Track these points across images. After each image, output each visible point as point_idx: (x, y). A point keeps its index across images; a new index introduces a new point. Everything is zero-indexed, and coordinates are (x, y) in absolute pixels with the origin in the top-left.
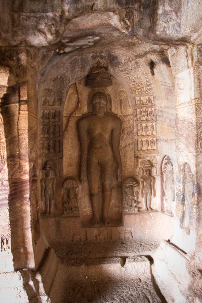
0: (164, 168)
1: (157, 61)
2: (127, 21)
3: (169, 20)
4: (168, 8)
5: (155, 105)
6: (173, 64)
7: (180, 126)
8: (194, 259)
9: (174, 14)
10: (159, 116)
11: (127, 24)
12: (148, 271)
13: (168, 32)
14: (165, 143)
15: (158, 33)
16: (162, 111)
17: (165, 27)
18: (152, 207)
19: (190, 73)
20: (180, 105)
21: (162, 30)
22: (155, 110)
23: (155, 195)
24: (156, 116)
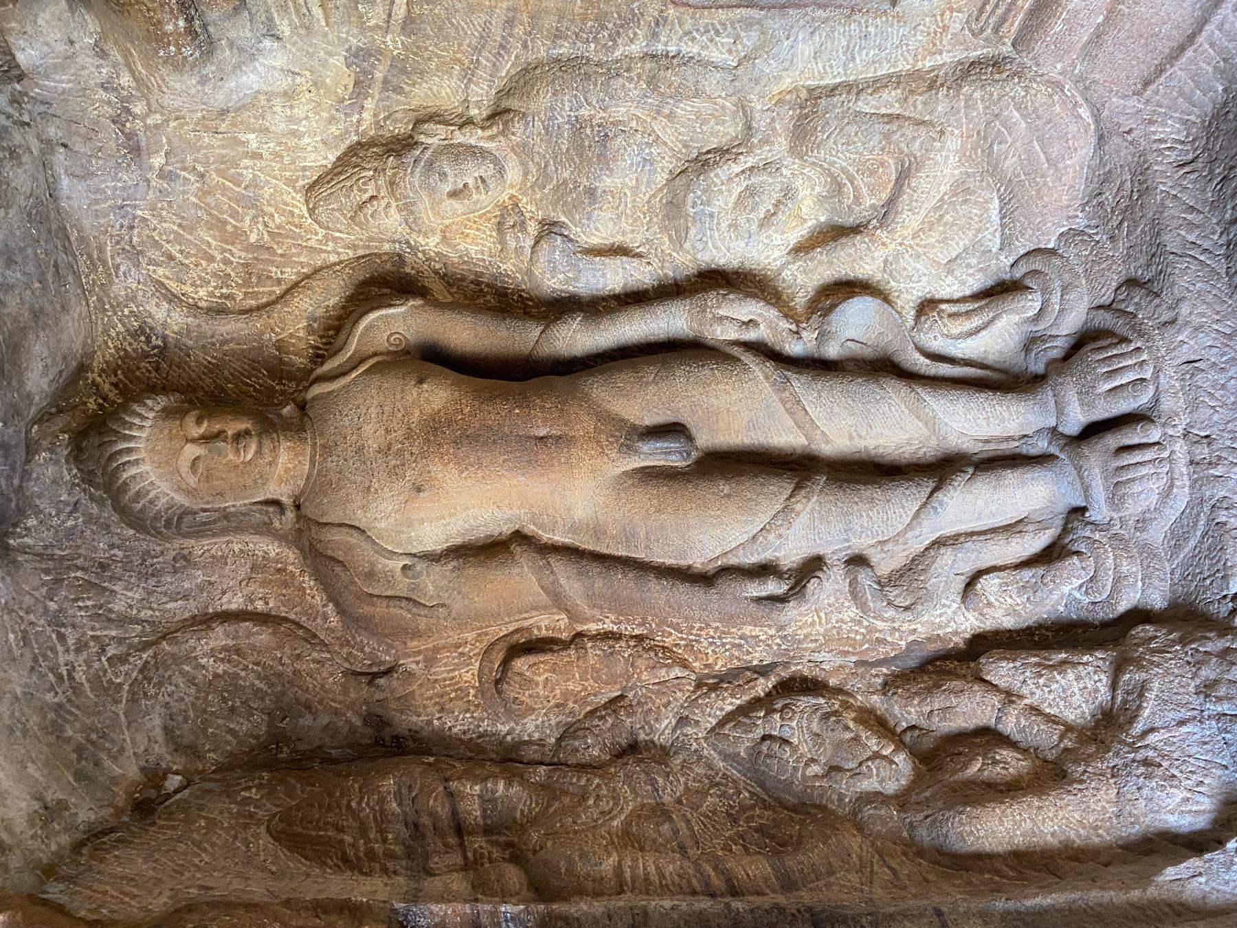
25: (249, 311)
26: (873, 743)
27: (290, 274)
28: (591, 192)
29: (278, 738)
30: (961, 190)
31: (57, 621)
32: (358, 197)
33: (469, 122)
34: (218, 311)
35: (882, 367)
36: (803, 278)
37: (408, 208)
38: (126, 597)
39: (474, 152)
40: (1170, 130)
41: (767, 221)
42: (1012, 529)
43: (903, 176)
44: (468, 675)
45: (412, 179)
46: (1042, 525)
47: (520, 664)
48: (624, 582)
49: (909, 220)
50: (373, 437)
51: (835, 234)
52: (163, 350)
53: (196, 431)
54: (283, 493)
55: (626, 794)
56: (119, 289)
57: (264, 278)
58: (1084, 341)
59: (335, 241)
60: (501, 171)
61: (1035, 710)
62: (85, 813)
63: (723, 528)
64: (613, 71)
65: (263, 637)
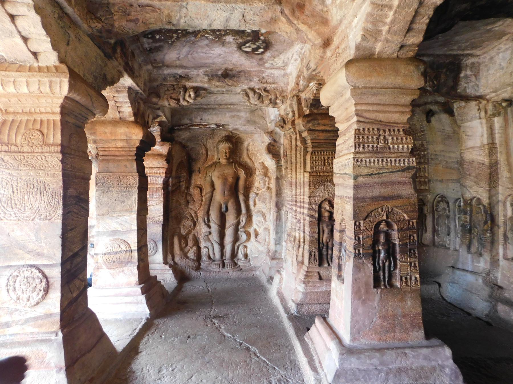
0: (436, 206)
1: (438, 111)
2: (435, 81)
3: (469, 81)
4: (469, 73)
5: (427, 149)
6: (458, 114)
7: (467, 167)
8: (489, 275)
9: (473, 77)
10: (432, 159)
11: (433, 83)
12: (437, 292)
13: (468, 91)
14: (438, 183)
15: (459, 91)
16: (436, 155)
17: (465, 87)
18: (423, 242)
19: (481, 123)
20: (468, 149)
21: (463, 89)
22: (428, 153)
23: (426, 231)
24: (428, 159)
25: (248, 154)
26: (187, 231)
27: (253, 159)
28: (260, 200)
29: (192, 159)
30: (259, 251)
31: (206, 135)
32: (260, 169)
33: (269, 184)
34: (248, 150)
35: (236, 239)
36: (251, 230)
37: (258, 175)
38: (210, 141)
39: (265, 185)
40: (258, 273)
41: (257, 224)
42: (214, 253)
43: (260, 242)
44: (199, 183)
45: (261, 177)
46: (214, 257)
47: (199, 189)
48: (208, 202)
49: (256, 244)
50: (226, 172)
51: (257, 235)
52: (242, 143)
53: (227, 151)
54: (221, 160)
55: (183, 202)
56: (248, 139)
57: (253, 156)
58: (236, 264)
59: (257, 166)
60: (263, 188)
61: (189, 250)
62: (183, 142)
63: (214, 215)
64: (270, 203)
65: (204, 157)
